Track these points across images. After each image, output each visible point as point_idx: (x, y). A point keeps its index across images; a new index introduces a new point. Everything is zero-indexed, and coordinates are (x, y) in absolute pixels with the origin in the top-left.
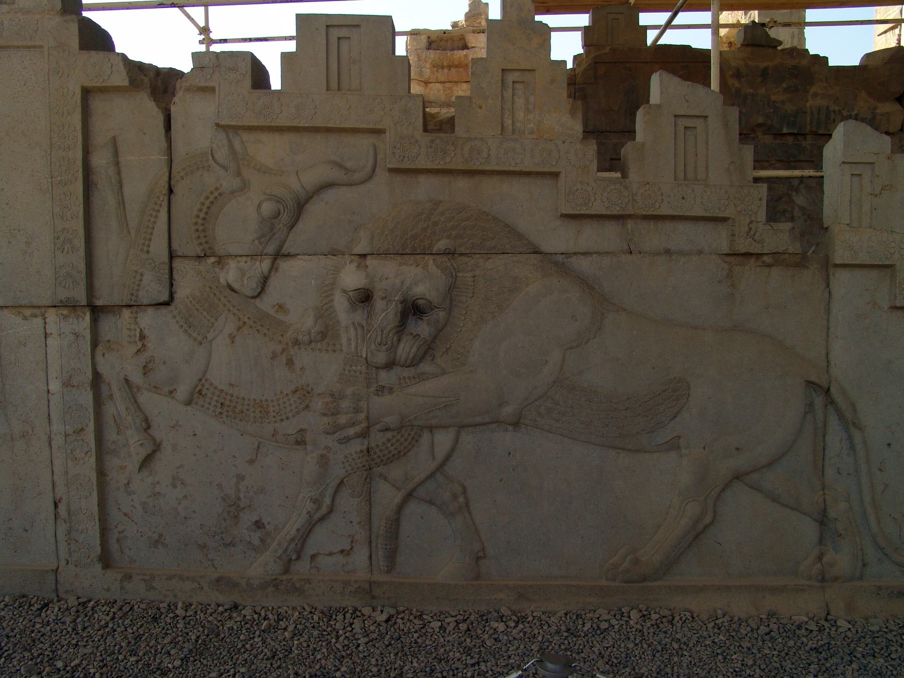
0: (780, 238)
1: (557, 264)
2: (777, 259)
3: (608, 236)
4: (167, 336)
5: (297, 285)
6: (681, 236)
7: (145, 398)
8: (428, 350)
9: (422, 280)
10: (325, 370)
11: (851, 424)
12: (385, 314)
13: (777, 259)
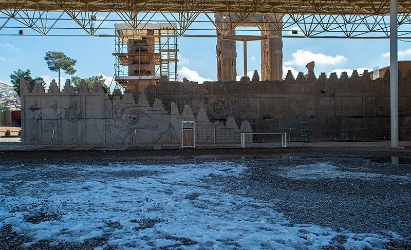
0: (166, 112)
1: (146, 115)
2: (166, 114)
3: (151, 112)
4: (112, 121)
5: (124, 117)
6: (157, 112)
7: (110, 127)
8: (136, 122)
9: (135, 116)
10: (126, 124)
11: (174, 128)
12: (132, 119)
13: (166, 114)
